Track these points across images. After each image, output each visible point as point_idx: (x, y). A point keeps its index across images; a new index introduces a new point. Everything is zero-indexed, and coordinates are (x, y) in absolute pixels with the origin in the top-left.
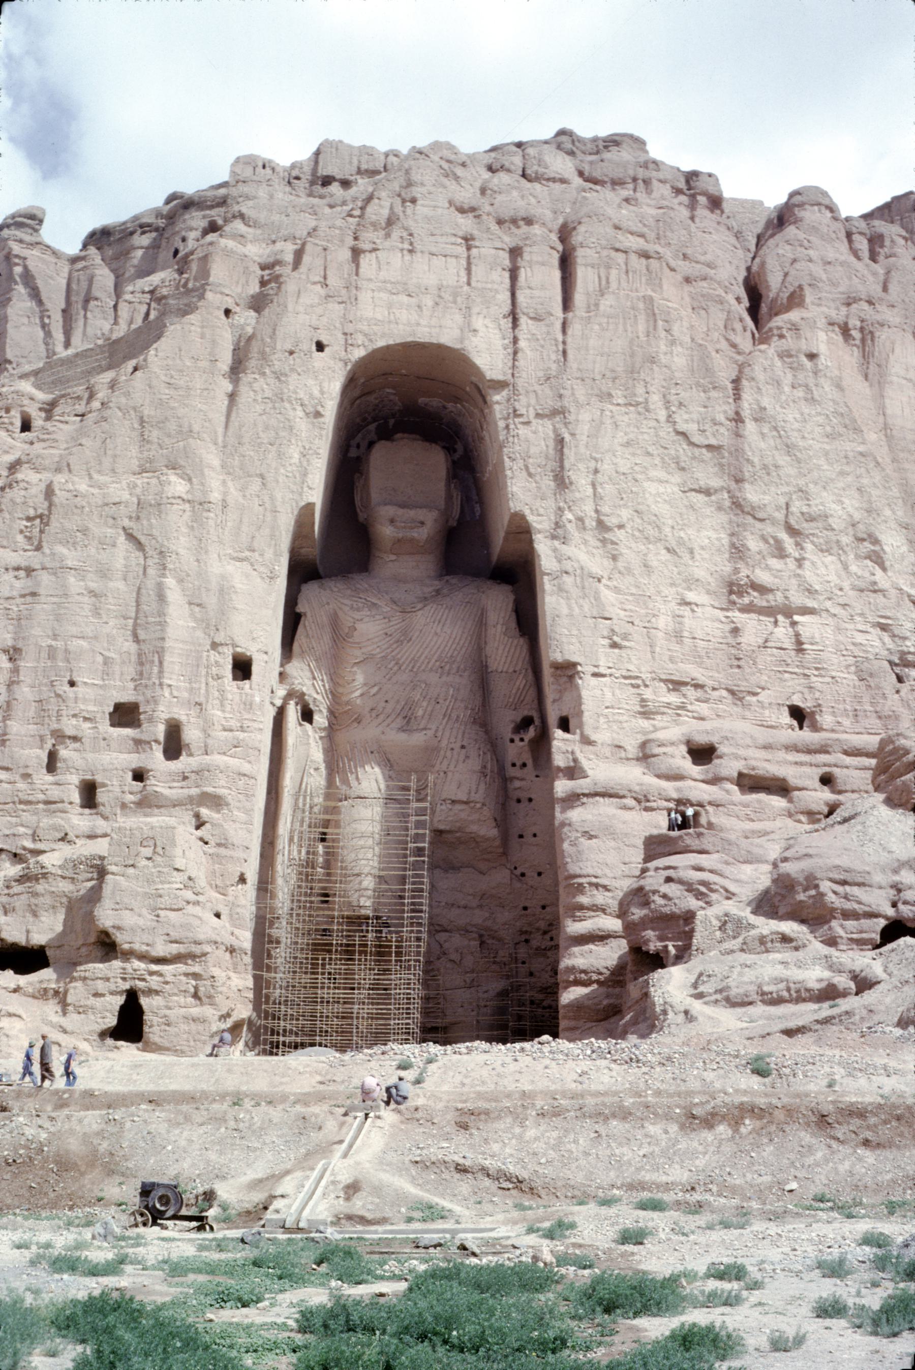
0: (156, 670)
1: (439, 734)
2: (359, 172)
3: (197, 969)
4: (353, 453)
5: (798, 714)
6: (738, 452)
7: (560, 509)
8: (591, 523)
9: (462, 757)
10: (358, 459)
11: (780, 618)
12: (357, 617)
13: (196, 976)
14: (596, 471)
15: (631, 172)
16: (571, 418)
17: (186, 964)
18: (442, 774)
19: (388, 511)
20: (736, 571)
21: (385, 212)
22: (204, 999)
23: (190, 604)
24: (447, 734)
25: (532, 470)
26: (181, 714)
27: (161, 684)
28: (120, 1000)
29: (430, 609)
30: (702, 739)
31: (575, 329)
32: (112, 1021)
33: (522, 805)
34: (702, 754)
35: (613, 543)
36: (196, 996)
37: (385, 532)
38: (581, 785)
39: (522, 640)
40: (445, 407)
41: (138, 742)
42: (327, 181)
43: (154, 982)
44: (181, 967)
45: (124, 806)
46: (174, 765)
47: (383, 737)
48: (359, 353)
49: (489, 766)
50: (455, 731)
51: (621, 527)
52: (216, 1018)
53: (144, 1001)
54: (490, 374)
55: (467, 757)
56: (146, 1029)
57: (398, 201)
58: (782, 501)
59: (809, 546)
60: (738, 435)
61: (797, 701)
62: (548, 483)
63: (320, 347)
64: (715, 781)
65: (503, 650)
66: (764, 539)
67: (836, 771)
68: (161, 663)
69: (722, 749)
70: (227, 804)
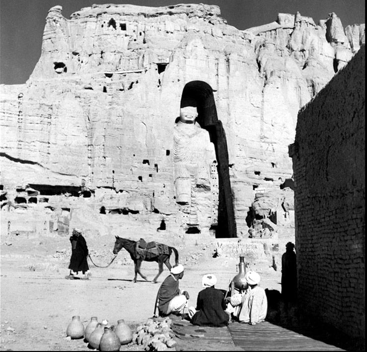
0: (152, 153)
2: (175, 30)
5: (273, 164)
6: (262, 109)
11: (270, 145)
15: (232, 33)
16: (230, 100)
20: (261, 134)
21: (190, 49)
28: (161, 222)
30: (257, 171)
31: (230, 78)
32: (159, 226)
34: (257, 173)
38: (236, 180)
41: (150, 168)
42: (167, 32)
43: (167, 219)
45: (148, 182)
46: (157, 173)
48: (187, 82)
53: (165, 222)
54: (213, 89)
56: (166, 228)
57: (193, 46)
58: (271, 119)
59: (275, 129)
60: (263, 105)
61: (273, 162)
62: (226, 114)
63: (179, 80)
64: (260, 179)
66: (267, 127)
67: (282, 177)
69: (261, 173)
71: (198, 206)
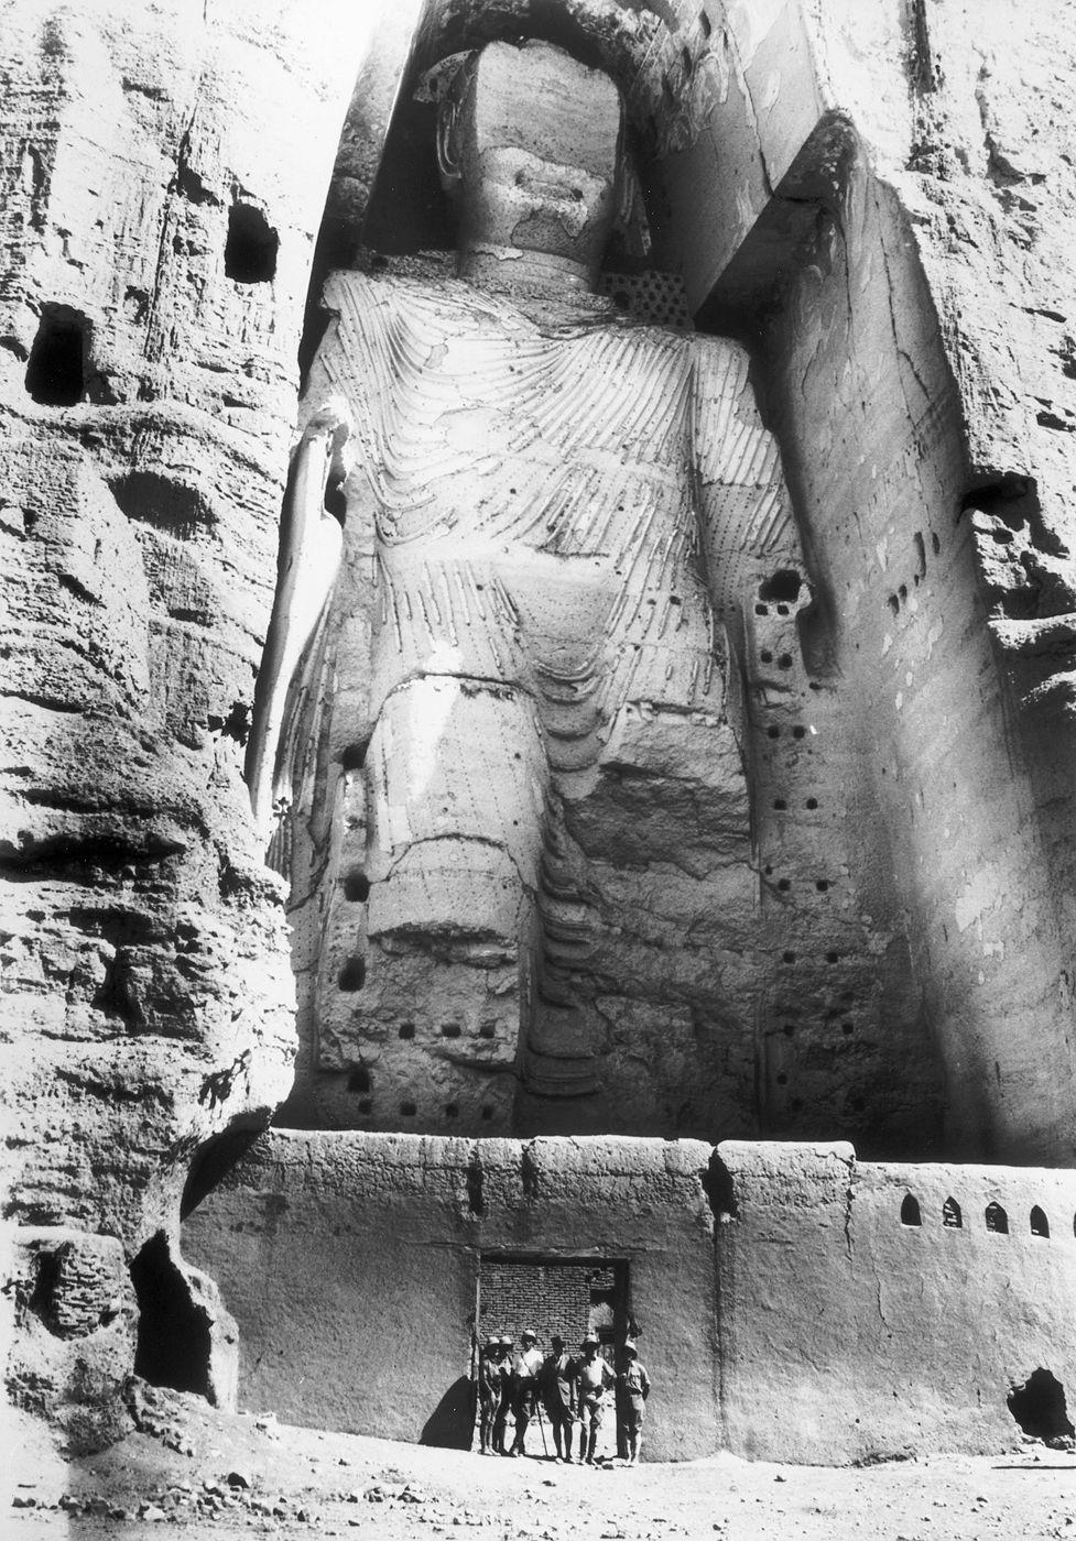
1: (627, 566)
3: (126, 898)
4: (422, 97)
7: (921, 123)
8: (979, 162)
9: (673, 623)
10: (432, 106)
12: (446, 328)
13: (122, 926)
14: (984, 74)
17: (87, 881)
18: (630, 649)
19: (513, 158)
22: (145, 1011)
23: (128, 86)
24: (642, 567)
25: (861, 47)
26: (85, 295)
27: (38, 222)
29: (599, 340)
33: (781, 743)
35: (1025, 206)
36: (114, 998)
37: (507, 197)
39: (768, 436)
40: (615, 23)
44: (64, 894)
47: (506, 559)
49: (727, 648)
50: (657, 569)
51: (1038, 179)
52: (196, 1082)
55: (684, 621)
65: (736, 448)
68: (40, 177)
70: (211, 519)
71: (611, 1006)
